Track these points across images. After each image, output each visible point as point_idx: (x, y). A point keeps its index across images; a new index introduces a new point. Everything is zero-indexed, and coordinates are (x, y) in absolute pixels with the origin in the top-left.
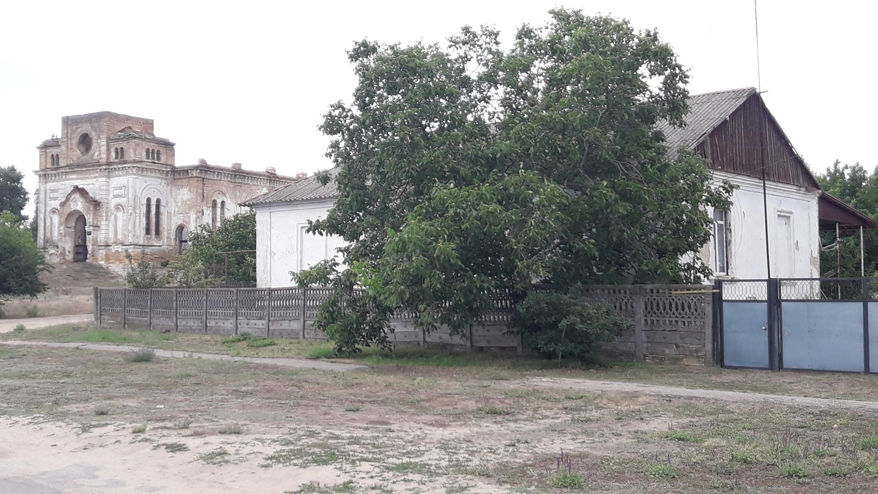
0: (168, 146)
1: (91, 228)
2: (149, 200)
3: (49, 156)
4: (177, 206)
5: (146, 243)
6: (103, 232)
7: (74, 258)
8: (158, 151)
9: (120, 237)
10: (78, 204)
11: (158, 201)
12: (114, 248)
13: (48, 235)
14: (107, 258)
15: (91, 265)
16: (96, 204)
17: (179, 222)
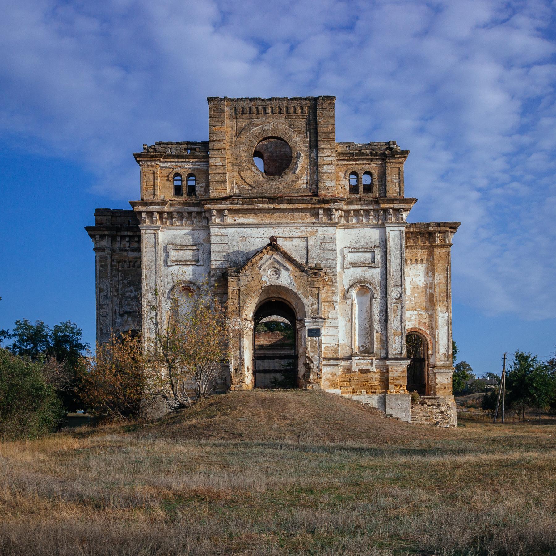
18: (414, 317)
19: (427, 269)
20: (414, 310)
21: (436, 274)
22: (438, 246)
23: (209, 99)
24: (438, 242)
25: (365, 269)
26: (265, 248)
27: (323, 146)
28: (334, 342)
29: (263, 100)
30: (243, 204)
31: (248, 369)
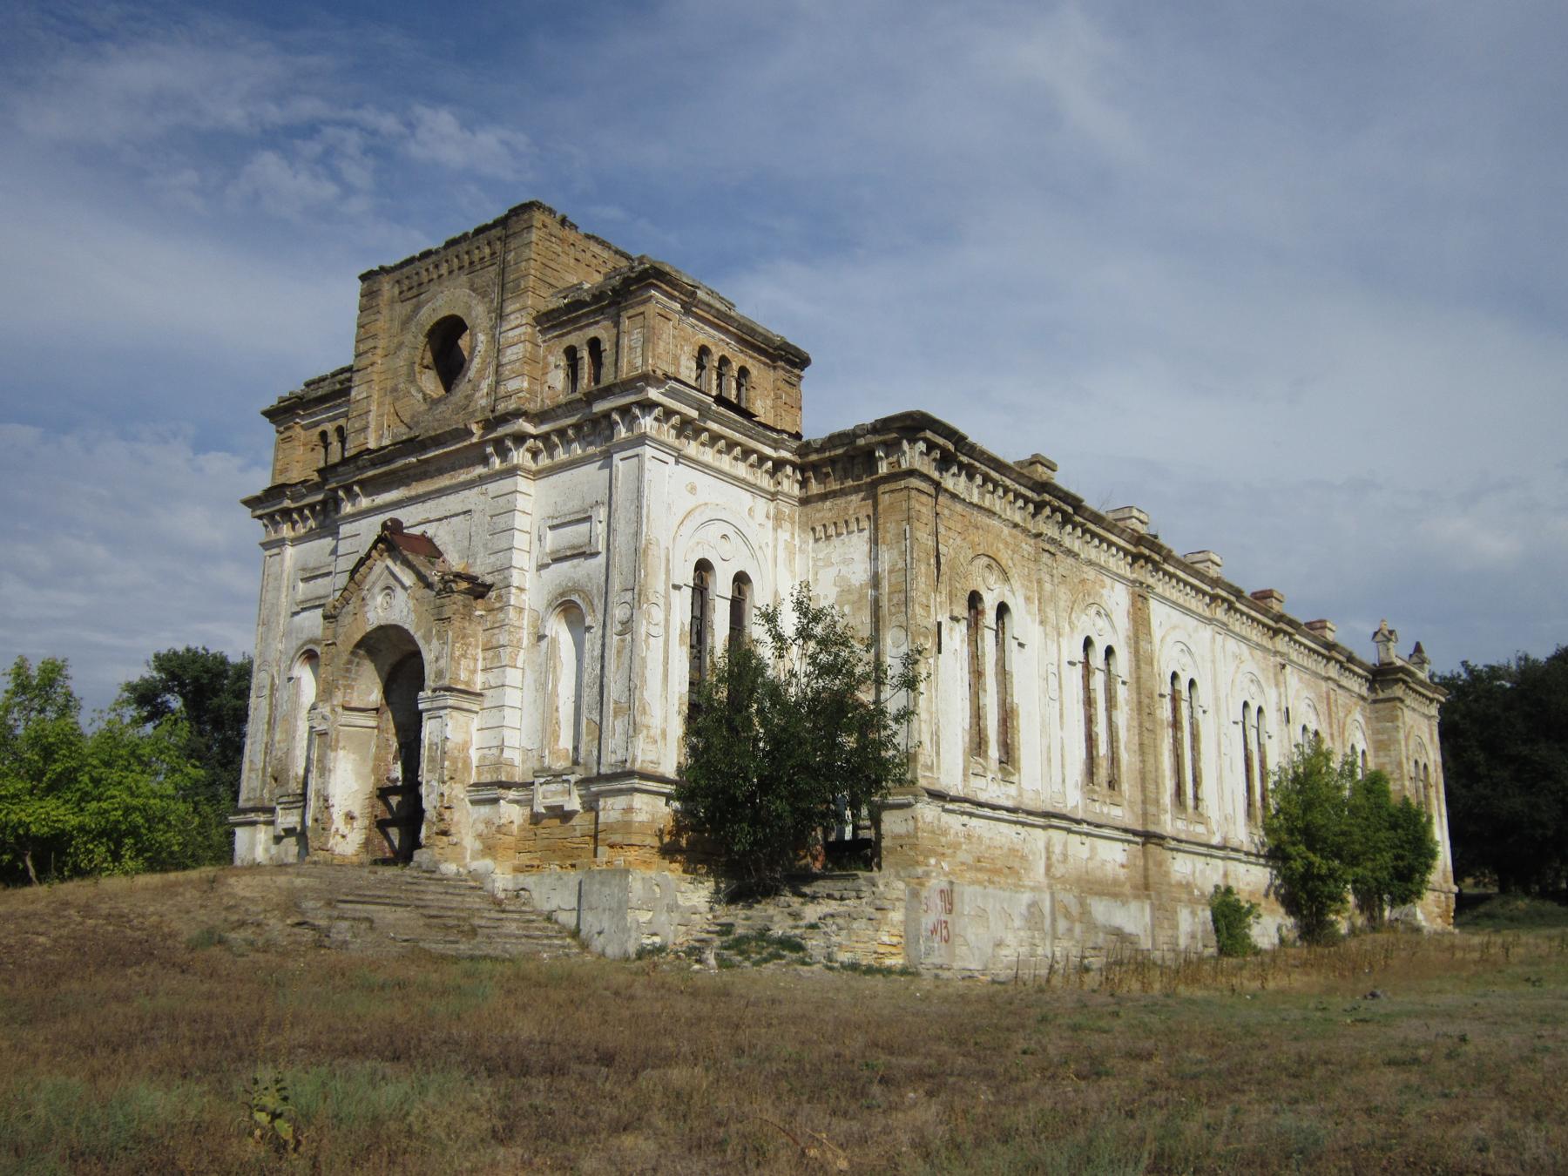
2: (703, 567)
8: (743, 372)
21: (883, 548)
24: (883, 468)
25: (575, 561)
26: (374, 546)
28: (495, 743)
29: (437, 252)
31: (350, 817)
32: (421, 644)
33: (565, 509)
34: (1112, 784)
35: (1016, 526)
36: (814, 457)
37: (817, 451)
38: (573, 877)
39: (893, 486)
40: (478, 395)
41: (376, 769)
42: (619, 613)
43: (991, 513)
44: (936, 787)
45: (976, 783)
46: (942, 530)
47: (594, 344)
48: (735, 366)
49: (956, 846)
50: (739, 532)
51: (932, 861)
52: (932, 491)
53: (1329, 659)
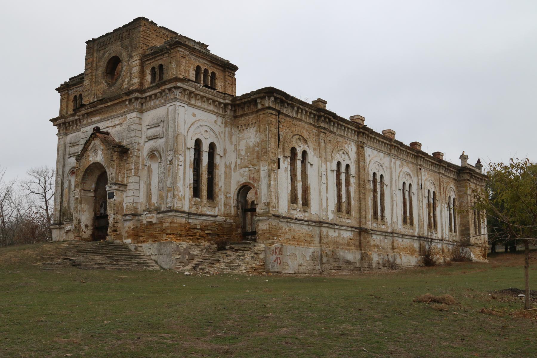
0: (229, 69)
1: (114, 187)
2: (198, 143)
3: (72, 98)
4: (239, 155)
5: (194, 210)
6: (130, 193)
7: (93, 235)
8: (213, 74)
9: (154, 200)
10: (98, 156)
11: (212, 146)
12: (146, 219)
13: (65, 204)
14: (136, 234)
15: (111, 244)
16: (122, 152)
17: (243, 180)
18: (246, 173)
19: (256, 131)
20: (246, 167)
22: (261, 110)
23: (87, 42)
24: (260, 107)
25: (156, 140)
27: (133, 54)
30: (91, 108)
31: (86, 226)
32: (106, 168)
33: (152, 123)
34: (349, 212)
35: (311, 124)
36: (238, 102)
37: (239, 100)
38: (156, 245)
39: (263, 112)
40: (124, 84)
41: (95, 211)
42: (170, 158)
43: (301, 120)
44: (277, 213)
45: (293, 212)
46: (281, 126)
47: (161, 66)
48: (210, 72)
49: (285, 233)
50: (211, 129)
51: (275, 238)
52: (277, 114)
53: (440, 166)
